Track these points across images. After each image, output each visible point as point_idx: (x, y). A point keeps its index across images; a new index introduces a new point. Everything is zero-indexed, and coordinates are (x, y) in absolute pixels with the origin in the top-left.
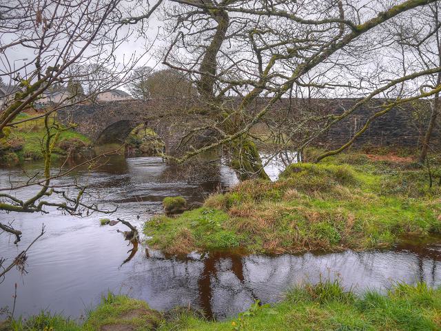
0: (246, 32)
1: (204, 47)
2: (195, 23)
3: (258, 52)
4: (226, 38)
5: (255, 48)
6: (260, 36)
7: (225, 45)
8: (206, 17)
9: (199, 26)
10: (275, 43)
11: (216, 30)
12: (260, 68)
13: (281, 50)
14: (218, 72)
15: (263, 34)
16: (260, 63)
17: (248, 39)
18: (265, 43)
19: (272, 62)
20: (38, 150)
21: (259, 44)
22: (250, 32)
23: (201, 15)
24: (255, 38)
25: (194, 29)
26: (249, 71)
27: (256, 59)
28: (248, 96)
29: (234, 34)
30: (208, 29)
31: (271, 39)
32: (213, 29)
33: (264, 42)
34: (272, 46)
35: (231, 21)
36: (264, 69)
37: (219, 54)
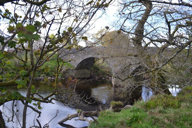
0: (162, 12)
1: (137, 20)
2: (134, 7)
3: (168, 23)
4: (150, 15)
5: (167, 21)
6: (170, 15)
7: (149, 19)
8: (140, 4)
9: (137, 9)
10: (179, 18)
11: (145, 11)
12: (170, 32)
13: (183, 22)
14: (144, 34)
15: (172, 13)
16: (170, 29)
17: (163, 16)
18: (173, 18)
19: (176, 29)
20: (24, 65)
21: (169, 19)
22: (164, 13)
23: (137, 3)
24: (167, 16)
25: (133, 11)
26: (163, 34)
27: (167, 27)
28: (161, 47)
29: (155, 13)
30: (141, 11)
31: (175, 16)
32: (143, 11)
33: (173, 18)
34: (178, 20)
35: (153, 6)
36: (171, 33)
37: (146, 24)
